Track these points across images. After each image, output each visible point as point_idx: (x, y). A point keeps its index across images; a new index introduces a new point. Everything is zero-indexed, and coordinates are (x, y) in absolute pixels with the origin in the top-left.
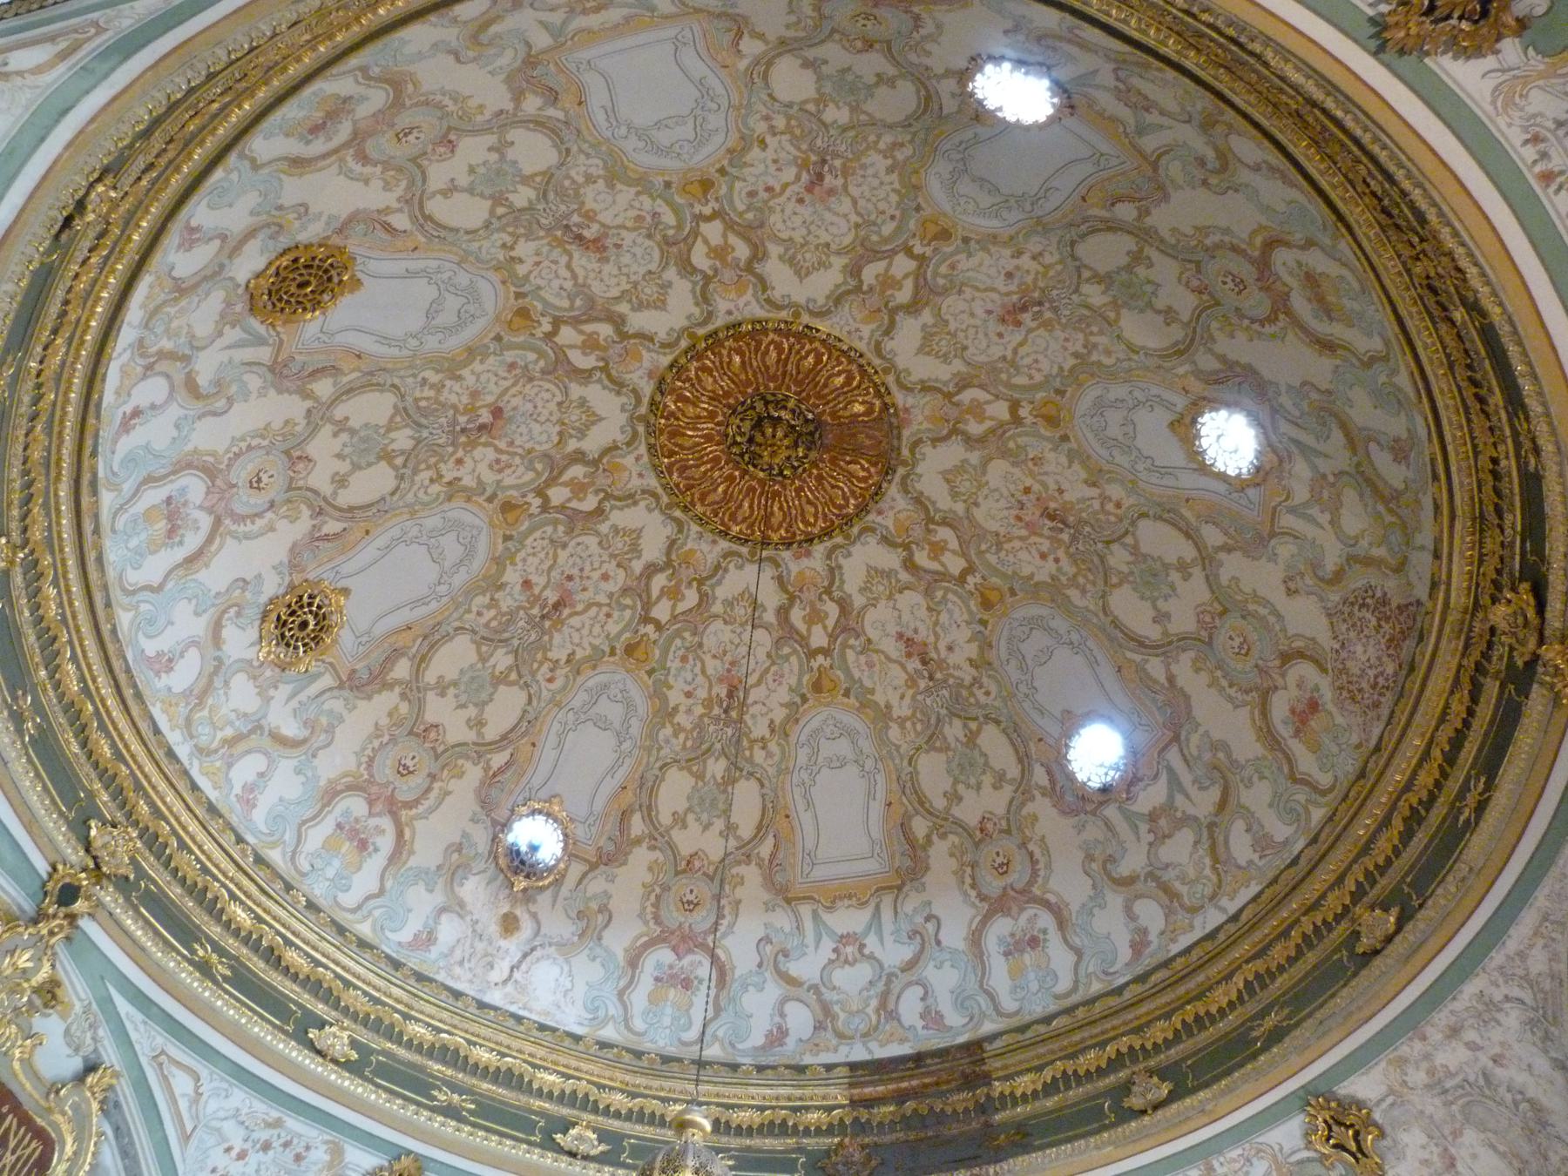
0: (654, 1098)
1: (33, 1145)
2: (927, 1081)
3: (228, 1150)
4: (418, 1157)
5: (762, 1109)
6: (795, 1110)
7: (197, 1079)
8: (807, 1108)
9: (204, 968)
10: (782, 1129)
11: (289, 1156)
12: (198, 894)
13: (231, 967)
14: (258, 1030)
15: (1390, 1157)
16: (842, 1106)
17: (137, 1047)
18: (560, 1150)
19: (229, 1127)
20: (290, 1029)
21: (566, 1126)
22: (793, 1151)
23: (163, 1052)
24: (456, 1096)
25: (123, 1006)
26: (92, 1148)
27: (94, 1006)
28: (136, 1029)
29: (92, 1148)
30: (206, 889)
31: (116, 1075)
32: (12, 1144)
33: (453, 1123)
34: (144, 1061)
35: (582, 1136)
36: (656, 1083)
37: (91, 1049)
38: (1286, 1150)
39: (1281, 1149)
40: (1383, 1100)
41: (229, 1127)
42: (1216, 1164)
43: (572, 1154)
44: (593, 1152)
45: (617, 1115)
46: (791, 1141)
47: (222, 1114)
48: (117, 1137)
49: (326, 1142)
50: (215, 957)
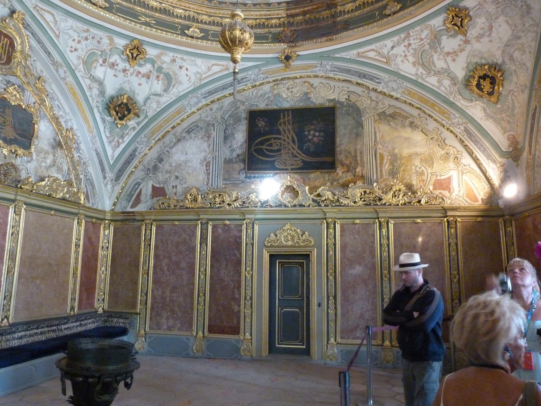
0: (218, 17)
1: (6, 40)
2: (314, 7)
5: (256, 19)
6: (267, 19)
7: (53, 16)
8: (272, 18)
10: (263, 26)
11: (95, 41)
15: (471, 27)
16: (284, 17)
18: (187, 36)
19: (71, 32)
21: (188, 28)
22: (267, 33)
24: (147, 19)
26: (27, 41)
29: (27, 41)
31: (23, 14)
33: (149, 28)
34: (31, 9)
35: (194, 30)
36: (218, 12)
37: (10, 5)
38: (436, 27)
39: (435, 26)
40: (475, 7)
41: (71, 32)
42: (411, 32)
43: (192, 37)
44: (199, 36)
45: (205, 23)
46: (266, 30)
47: (67, 28)
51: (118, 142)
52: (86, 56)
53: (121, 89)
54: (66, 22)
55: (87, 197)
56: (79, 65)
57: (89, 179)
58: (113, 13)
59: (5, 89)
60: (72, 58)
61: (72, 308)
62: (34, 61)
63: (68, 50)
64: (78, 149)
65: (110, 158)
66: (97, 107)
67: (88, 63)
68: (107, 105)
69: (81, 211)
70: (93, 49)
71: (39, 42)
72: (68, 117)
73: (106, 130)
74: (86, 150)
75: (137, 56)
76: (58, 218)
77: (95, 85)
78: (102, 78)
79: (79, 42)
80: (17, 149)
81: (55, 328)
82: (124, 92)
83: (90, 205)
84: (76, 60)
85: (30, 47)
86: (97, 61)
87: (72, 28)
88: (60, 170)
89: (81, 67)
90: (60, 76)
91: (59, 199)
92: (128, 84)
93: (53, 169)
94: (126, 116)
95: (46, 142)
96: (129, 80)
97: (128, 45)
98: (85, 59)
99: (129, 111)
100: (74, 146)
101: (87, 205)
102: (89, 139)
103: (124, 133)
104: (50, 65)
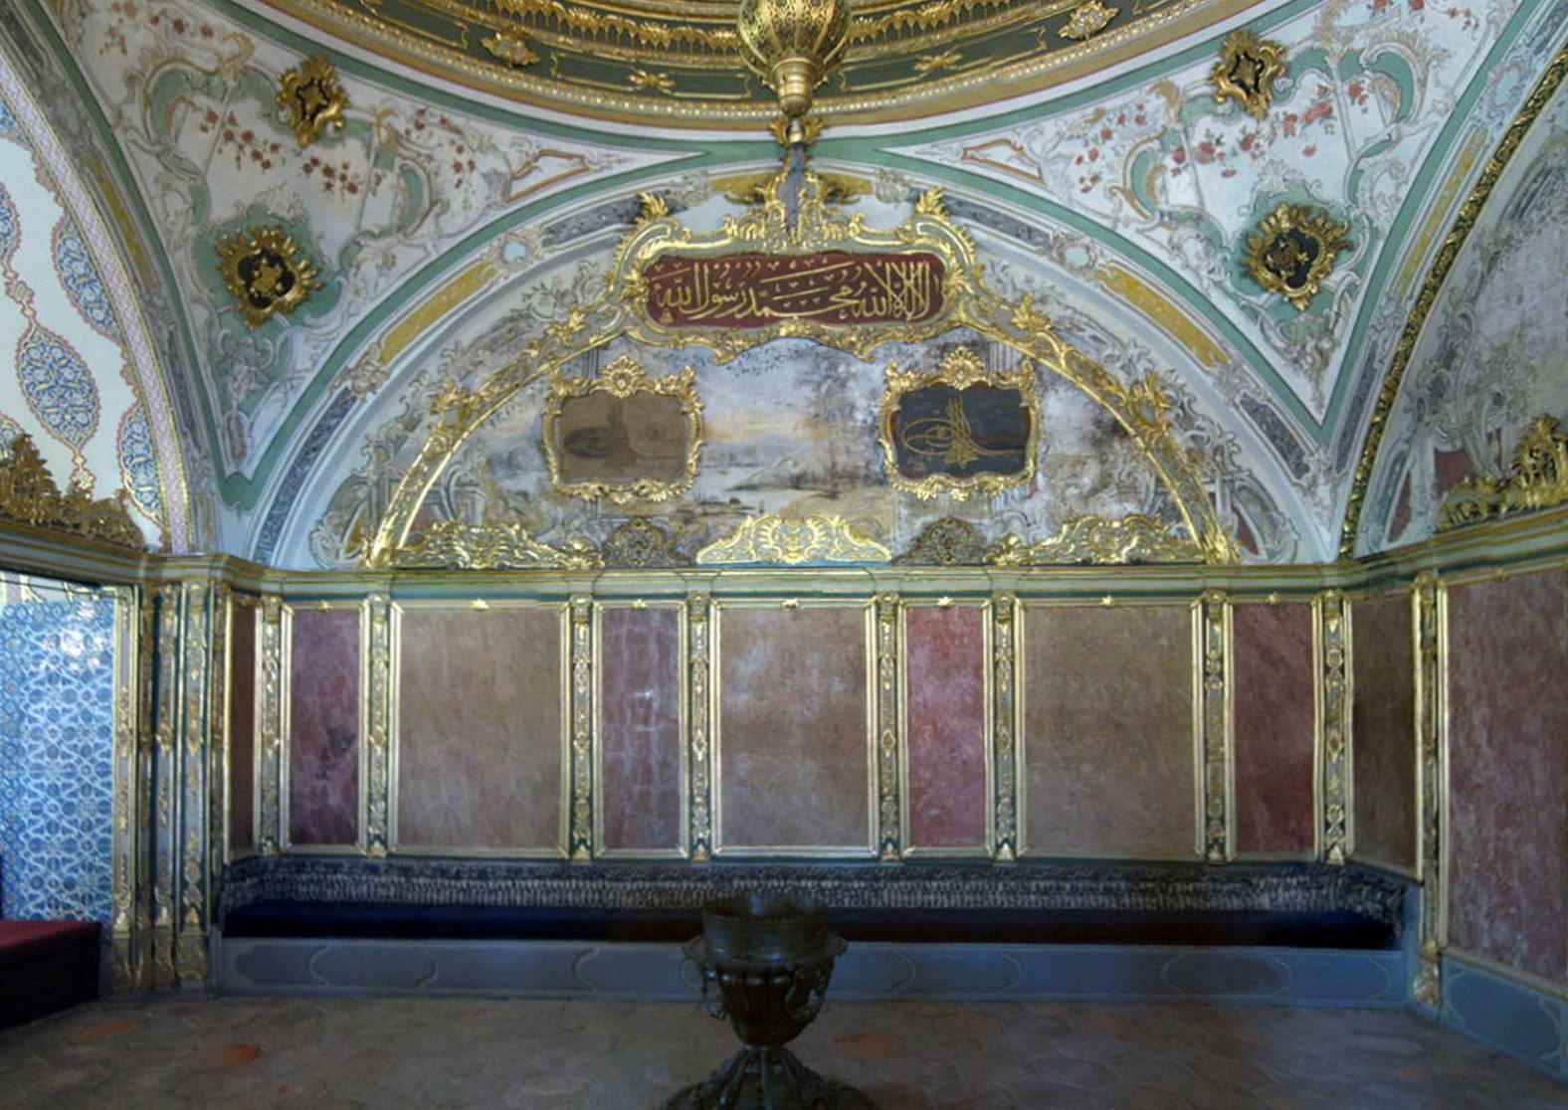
1: (920, 265)
3: (1080, 160)
4: (1238, 31)
7: (1007, 142)
9: (938, 73)
12: (891, 35)
13: (955, 53)
14: (1015, 73)
17: (945, 163)
20: (1043, 46)
23: (966, 150)
25: (909, 151)
27: (887, 169)
28: (932, 154)
30: (891, 26)
32: (903, 275)
34: (958, 165)
41: (1064, 148)
47: (1050, 146)
48: (978, 220)
49: (1151, 90)
50: (937, 59)
51: (1321, 352)
52: (1128, 176)
53: (1262, 198)
54: (1041, 133)
55: (1245, 537)
56: (1120, 210)
57: (1241, 488)
58: (1139, 17)
59: (938, 367)
60: (1097, 204)
61: (1216, 843)
62: (1004, 268)
63: (1077, 193)
64: (1187, 420)
65: (1311, 406)
66: (1218, 284)
67: (1140, 190)
68: (1239, 264)
69: (1211, 583)
70: (1138, 145)
71: (995, 221)
72: (1133, 352)
73: (1270, 333)
74: (1216, 411)
75: (1257, 79)
76: (1133, 611)
77: (1185, 232)
78: (1194, 203)
79: (1094, 155)
80: (986, 478)
81: (1150, 885)
82: (1272, 203)
83: (1263, 557)
84: (1106, 202)
85: (977, 246)
86: (1160, 168)
87: (1060, 136)
88: (1127, 490)
89: (1128, 210)
90: (1071, 268)
91: (1119, 564)
92: (1276, 172)
93: (1104, 495)
94: (1309, 265)
95: (1073, 438)
96: (1272, 161)
97: (1215, 68)
98: (1128, 186)
99: (1312, 248)
100: (1171, 416)
101: (1248, 560)
102: (1210, 381)
103: (1327, 319)
104: (1035, 257)
